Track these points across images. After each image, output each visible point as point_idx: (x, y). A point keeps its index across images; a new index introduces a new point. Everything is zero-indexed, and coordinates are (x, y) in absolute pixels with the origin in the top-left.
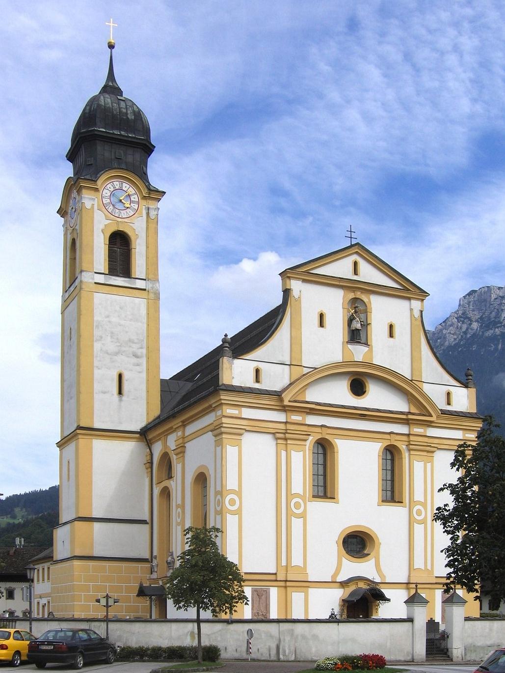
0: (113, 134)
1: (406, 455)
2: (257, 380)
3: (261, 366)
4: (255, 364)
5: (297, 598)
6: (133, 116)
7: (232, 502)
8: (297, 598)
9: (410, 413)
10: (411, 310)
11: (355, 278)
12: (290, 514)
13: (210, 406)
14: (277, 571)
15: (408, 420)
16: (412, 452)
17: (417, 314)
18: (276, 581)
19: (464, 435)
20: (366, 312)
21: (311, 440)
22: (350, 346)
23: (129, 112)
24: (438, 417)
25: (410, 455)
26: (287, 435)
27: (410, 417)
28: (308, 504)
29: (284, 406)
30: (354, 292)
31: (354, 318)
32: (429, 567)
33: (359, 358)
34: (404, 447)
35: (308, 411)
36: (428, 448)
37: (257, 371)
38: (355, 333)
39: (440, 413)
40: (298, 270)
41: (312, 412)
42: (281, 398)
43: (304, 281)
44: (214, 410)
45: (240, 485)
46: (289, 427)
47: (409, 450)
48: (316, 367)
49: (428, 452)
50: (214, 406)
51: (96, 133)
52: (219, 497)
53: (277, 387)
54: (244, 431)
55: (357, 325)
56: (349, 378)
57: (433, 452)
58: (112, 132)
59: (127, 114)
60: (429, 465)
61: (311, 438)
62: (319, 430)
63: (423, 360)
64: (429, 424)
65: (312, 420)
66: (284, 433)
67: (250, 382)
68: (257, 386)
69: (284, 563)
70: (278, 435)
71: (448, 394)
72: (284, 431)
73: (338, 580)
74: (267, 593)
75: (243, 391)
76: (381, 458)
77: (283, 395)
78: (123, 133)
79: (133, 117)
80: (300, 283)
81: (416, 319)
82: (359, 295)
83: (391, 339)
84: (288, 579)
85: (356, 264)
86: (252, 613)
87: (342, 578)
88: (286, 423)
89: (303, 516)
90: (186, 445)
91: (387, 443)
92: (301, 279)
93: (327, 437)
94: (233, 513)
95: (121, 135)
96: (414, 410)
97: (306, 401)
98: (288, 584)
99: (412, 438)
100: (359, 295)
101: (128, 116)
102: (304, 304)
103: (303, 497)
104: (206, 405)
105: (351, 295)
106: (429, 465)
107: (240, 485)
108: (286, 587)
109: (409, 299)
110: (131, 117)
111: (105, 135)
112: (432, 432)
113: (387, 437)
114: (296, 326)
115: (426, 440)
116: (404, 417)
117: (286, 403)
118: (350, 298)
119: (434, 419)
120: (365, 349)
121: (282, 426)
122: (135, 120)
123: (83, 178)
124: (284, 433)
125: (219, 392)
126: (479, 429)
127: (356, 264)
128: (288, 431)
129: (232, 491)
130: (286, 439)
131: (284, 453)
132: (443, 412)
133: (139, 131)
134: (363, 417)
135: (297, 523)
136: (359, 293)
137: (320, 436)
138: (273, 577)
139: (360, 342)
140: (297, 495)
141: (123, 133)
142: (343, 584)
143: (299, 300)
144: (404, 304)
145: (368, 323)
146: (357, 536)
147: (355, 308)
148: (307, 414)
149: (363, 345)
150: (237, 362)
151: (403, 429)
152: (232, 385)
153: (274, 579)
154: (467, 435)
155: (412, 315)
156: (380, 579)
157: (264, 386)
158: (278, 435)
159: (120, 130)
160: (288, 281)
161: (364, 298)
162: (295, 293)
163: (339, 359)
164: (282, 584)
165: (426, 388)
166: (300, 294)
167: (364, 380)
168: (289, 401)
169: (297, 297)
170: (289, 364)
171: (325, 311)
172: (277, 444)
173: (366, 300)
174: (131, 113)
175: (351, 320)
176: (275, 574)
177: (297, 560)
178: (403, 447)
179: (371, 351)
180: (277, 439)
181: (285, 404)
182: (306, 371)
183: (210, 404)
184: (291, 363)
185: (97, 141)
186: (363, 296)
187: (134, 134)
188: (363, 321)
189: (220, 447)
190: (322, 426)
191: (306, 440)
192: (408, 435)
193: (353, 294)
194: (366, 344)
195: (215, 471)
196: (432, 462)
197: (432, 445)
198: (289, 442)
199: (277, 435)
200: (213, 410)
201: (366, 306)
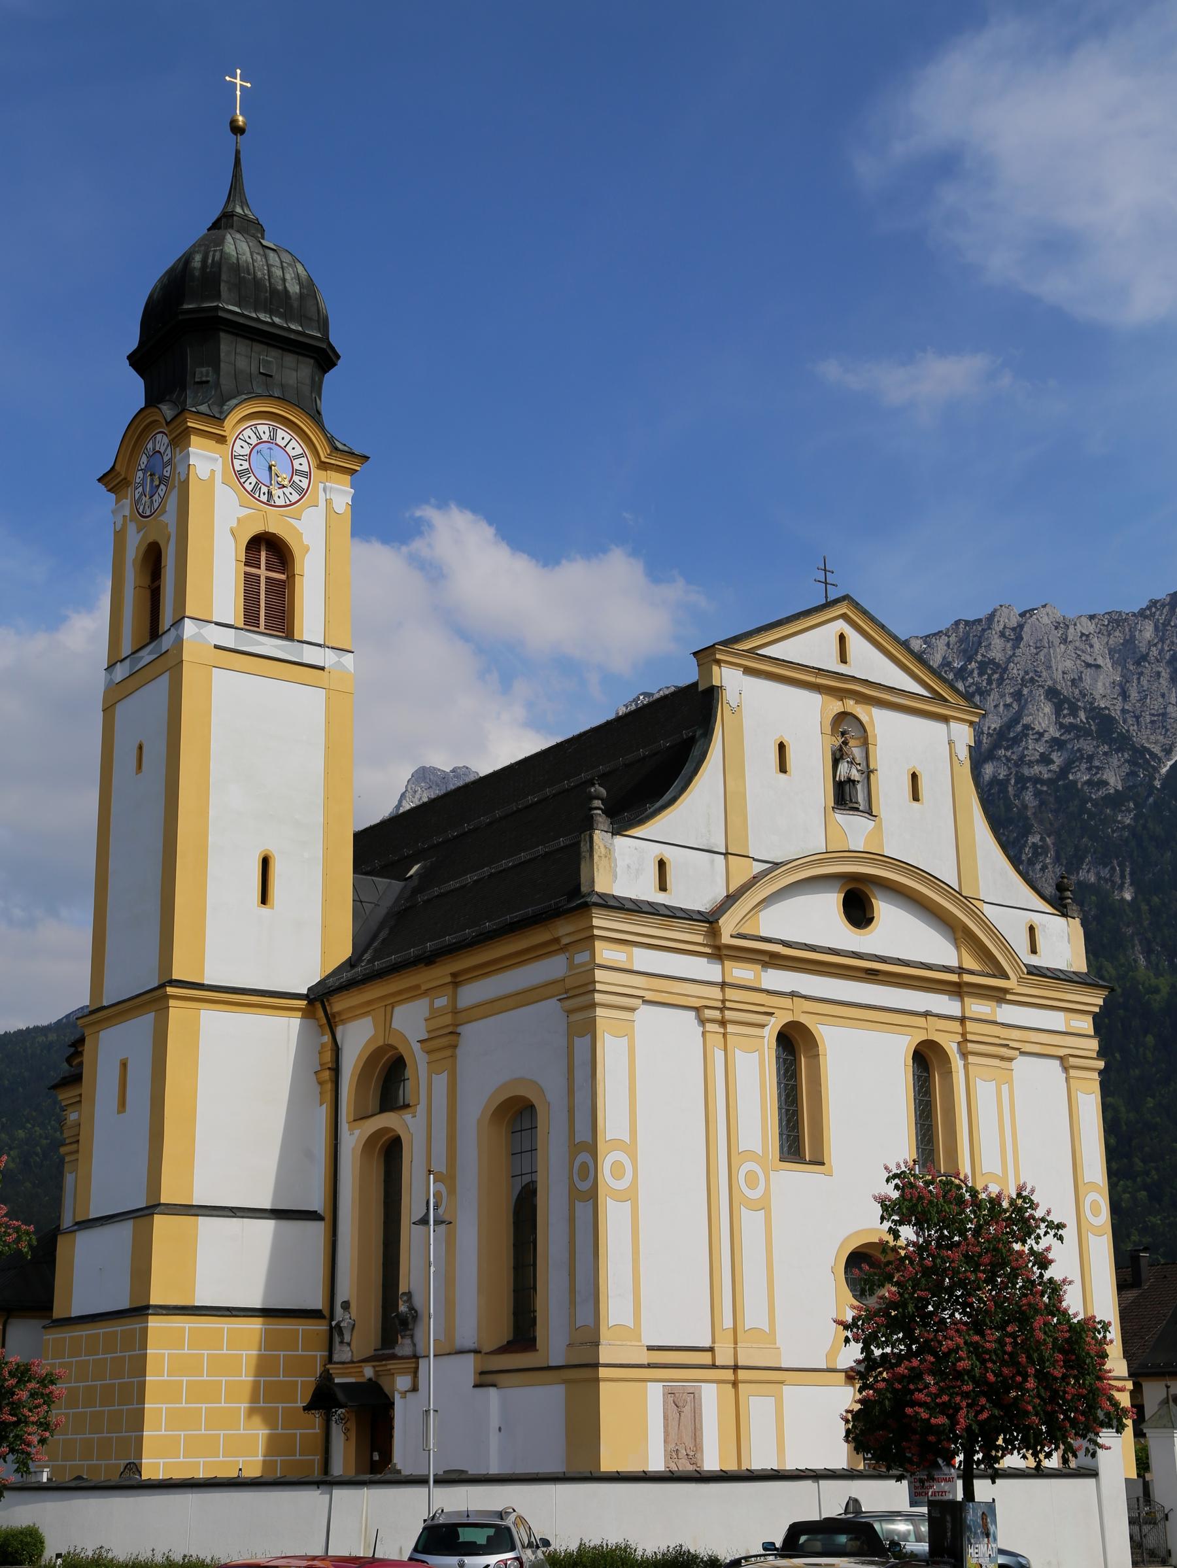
0: (258, 320)
1: (957, 1063)
2: (663, 888)
3: (669, 853)
4: (657, 850)
5: (759, 1407)
6: (298, 287)
8: (759, 1407)
9: (961, 970)
10: (951, 743)
13: (556, 940)
14: (714, 1341)
15: (959, 985)
16: (971, 1059)
18: (714, 1366)
19: (1067, 1023)
20: (865, 743)
22: (843, 819)
23: (288, 277)
25: (966, 1067)
26: (727, 1012)
27: (967, 978)
30: (842, 700)
33: (858, 844)
34: (954, 1046)
35: (767, 959)
36: (1003, 1051)
37: (662, 864)
38: (847, 787)
39: (1025, 970)
41: (772, 960)
42: (713, 928)
43: (748, 671)
44: (564, 949)
46: (731, 994)
47: (964, 1055)
48: (776, 861)
49: (1002, 1058)
50: (565, 941)
51: (221, 314)
52: (583, 1157)
53: (701, 902)
56: (839, 886)
57: (1011, 1059)
58: (254, 315)
59: (284, 280)
61: (772, 1020)
62: (786, 1002)
63: (980, 854)
64: (999, 996)
67: (644, 889)
69: (728, 1323)
70: (708, 1013)
71: (1032, 929)
72: (719, 1005)
74: (695, 1396)
75: (636, 908)
76: (910, 1069)
77: (721, 922)
80: (738, 673)
82: (851, 706)
83: (915, 804)
85: (842, 638)
86: (665, 1450)
88: (723, 985)
89: (763, 1205)
90: (459, 1030)
91: (921, 1036)
93: (804, 1019)
94: (621, 1197)
95: (273, 324)
96: (970, 963)
97: (761, 937)
98: (742, 1374)
99: (970, 1026)
101: (287, 285)
102: (748, 723)
104: (538, 936)
105: (836, 706)
106: (1005, 1088)
109: (945, 719)
110: (294, 288)
111: (242, 320)
112: (1007, 1013)
113: (921, 1021)
114: (732, 770)
116: (954, 978)
117: (726, 939)
118: (835, 712)
120: (869, 824)
121: (716, 993)
122: (302, 296)
123: (194, 409)
124: (722, 1010)
125: (591, 909)
126: (1097, 1010)
127: (842, 638)
128: (728, 1004)
129: (617, 1144)
130: (723, 1023)
131: (719, 1055)
132: (1034, 971)
133: (311, 319)
134: (871, 976)
135: (751, 1221)
136: (852, 702)
137: (787, 1018)
138: (706, 1358)
139: (857, 809)
140: (750, 1155)
141: (277, 320)
143: (736, 711)
144: (939, 727)
145: (872, 767)
147: (843, 734)
149: (867, 815)
150: (619, 840)
151: (950, 1006)
152: (614, 896)
153: (709, 1362)
154: (1073, 1023)
155: (952, 754)
157: (678, 897)
158: (708, 1013)
159: (271, 313)
160: (715, 668)
161: (860, 711)
163: (816, 843)
164: (728, 1375)
168: (732, 936)
169: (734, 704)
170: (724, 852)
172: (703, 1033)
173: (864, 718)
174: (292, 279)
176: (711, 1349)
177: (755, 1317)
178: (952, 1048)
179: (879, 828)
180: (702, 1022)
181: (723, 942)
182: (759, 867)
183: (556, 936)
184: (727, 848)
185: (222, 335)
186: (858, 709)
187: (301, 326)
188: (859, 764)
189: (588, 1037)
190: (793, 994)
191: (763, 1026)
192: (963, 1020)
194: (869, 812)
195: (571, 1092)
196: (1010, 1082)
197: (1012, 1044)
199: (707, 1011)
200: (562, 949)
201: (865, 731)
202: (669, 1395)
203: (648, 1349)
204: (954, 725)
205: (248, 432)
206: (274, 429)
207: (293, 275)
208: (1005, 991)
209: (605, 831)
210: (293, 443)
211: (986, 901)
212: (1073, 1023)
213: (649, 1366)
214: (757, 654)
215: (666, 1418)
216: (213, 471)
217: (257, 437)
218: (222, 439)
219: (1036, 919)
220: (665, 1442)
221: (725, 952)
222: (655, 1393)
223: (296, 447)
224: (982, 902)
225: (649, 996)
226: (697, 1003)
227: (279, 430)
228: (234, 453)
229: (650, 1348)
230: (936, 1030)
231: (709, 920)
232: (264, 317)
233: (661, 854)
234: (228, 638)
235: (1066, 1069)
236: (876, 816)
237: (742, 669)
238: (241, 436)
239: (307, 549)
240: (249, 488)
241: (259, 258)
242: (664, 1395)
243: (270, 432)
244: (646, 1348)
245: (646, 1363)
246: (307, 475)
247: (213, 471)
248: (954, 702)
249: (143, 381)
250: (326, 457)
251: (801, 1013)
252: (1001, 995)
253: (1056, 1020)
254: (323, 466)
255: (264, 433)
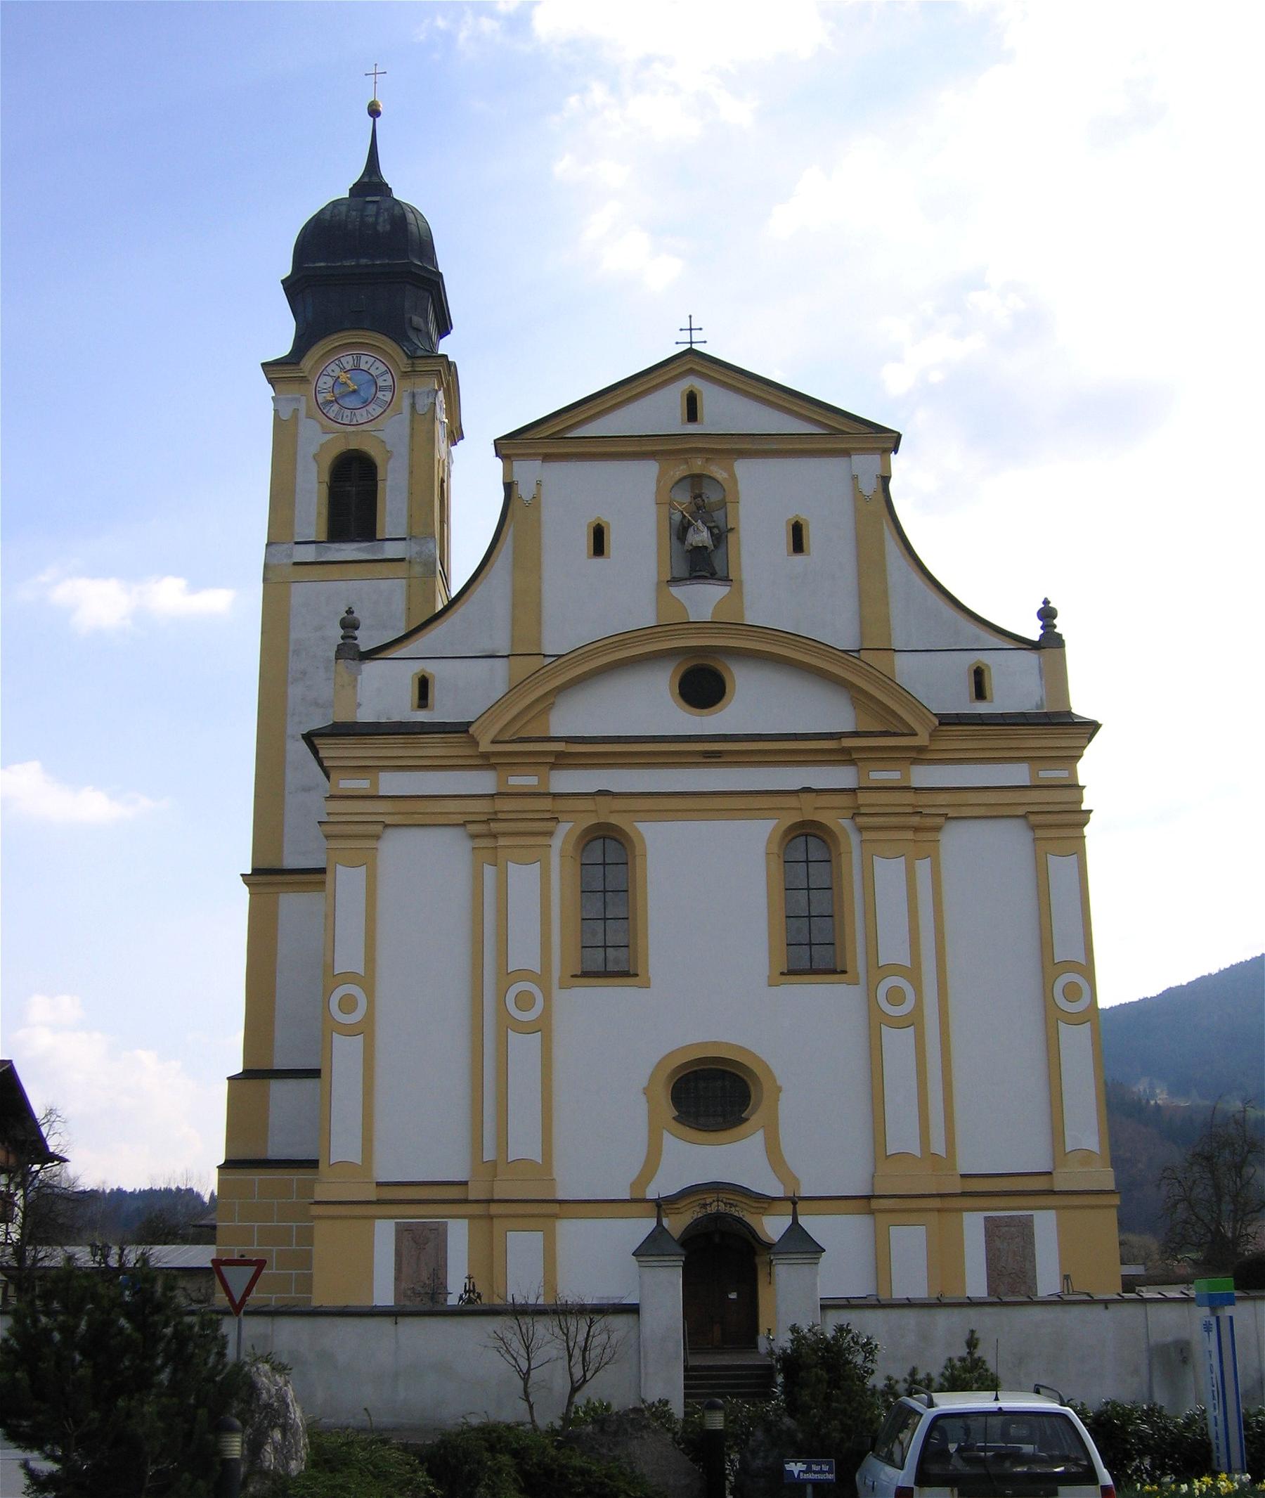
3: (430, 668)
4: (417, 667)
7: (348, 1004)
11: (692, 428)
12: (507, 1024)
15: (847, 751)
17: (869, 486)
18: (466, 1201)
21: (564, 833)
22: (675, 591)
24: (932, 736)
27: (847, 743)
28: (560, 996)
29: (486, 755)
31: (690, 524)
32: (938, 1147)
40: (528, 435)
41: (561, 761)
43: (547, 458)
45: (370, 960)
47: (861, 829)
49: (916, 829)
54: (379, 828)
55: (701, 536)
57: (937, 829)
60: (923, 867)
64: (919, 756)
65: (566, 781)
66: (487, 821)
67: (403, 709)
68: (422, 716)
72: (484, 818)
73: (649, 1197)
77: (471, 730)
78: (363, 261)
79: (388, 227)
81: (867, 499)
84: (496, 1197)
87: (664, 1185)
89: (543, 1027)
92: (539, 454)
93: (614, 820)
94: (349, 1031)
98: (495, 1209)
99: (863, 798)
100: (698, 465)
103: (542, 979)
105: (681, 471)
107: (370, 960)
108: (491, 1217)
109: (846, 453)
112: (923, 776)
113: (792, 802)
115: (909, 798)
117: (485, 746)
119: (922, 739)
128: (500, 816)
132: (946, 720)
135: (524, 1049)
140: (524, 974)
141: (363, 261)
142: (662, 1205)
146: (724, 1072)
148: (552, 769)
151: (842, 777)
154: (1042, 774)
155: (857, 493)
156: (782, 1187)
157: (442, 711)
162: (525, 491)
165: (907, 669)
166: (539, 490)
167: (719, 668)
168: (493, 742)
171: (606, 518)
174: (384, 221)
175: (682, 531)
176: (465, 1183)
178: (842, 824)
179: (738, 593)
191: (550, 834)
193: (683, 467)
194: (726, 580)
196: (935, 858)
197: (926, 811)
198: (502, 841)
202: (406, 1233)
203: (377, 1185)
204: (856, 458)
205: (333, 366)
206: (357, 357)
207: (386, 217)
208: (921, 749)
209: (350, 659)
210: (378, 364)
211: (897, 649)
212: (1065, 774)
213: (379, 1202)
214: (565, 438)
215: (398, 1254)
216: (296, 410)
217: (341, 368)
218: (304, 380)
219: (985, 658)
220: (396, 1279)
221: (493, 761)
222: (384, 1234)
223: (377, 369)
224: (892, 652)
225: (388, 820)
226: (460, 819)
227: (363, 356)
228: (318, 389)
229: (379, 1184)
230: (816, 808)
231: (461, 729)
232: (347, 263)
233: (423, 670)
234: (308, 554)
235: (1033, 828)
236: (732, 580)
237: (541, 458)
238: (324, 373)
239: (389, 455)
240: (332, 415)
241: (354, 213)
242: (397, 1231)
243: (354, 361)
244: (375, 1184)
245: (375, 1199)
246: (393, 389)
247: (296, 410)
248: (851, 432)
249: (287, 353)
250: (405, 367)
251: (607, 813)
252: (914, 755)
253: (1017, 774)
254: (405, 375)
255: (348, 363)
